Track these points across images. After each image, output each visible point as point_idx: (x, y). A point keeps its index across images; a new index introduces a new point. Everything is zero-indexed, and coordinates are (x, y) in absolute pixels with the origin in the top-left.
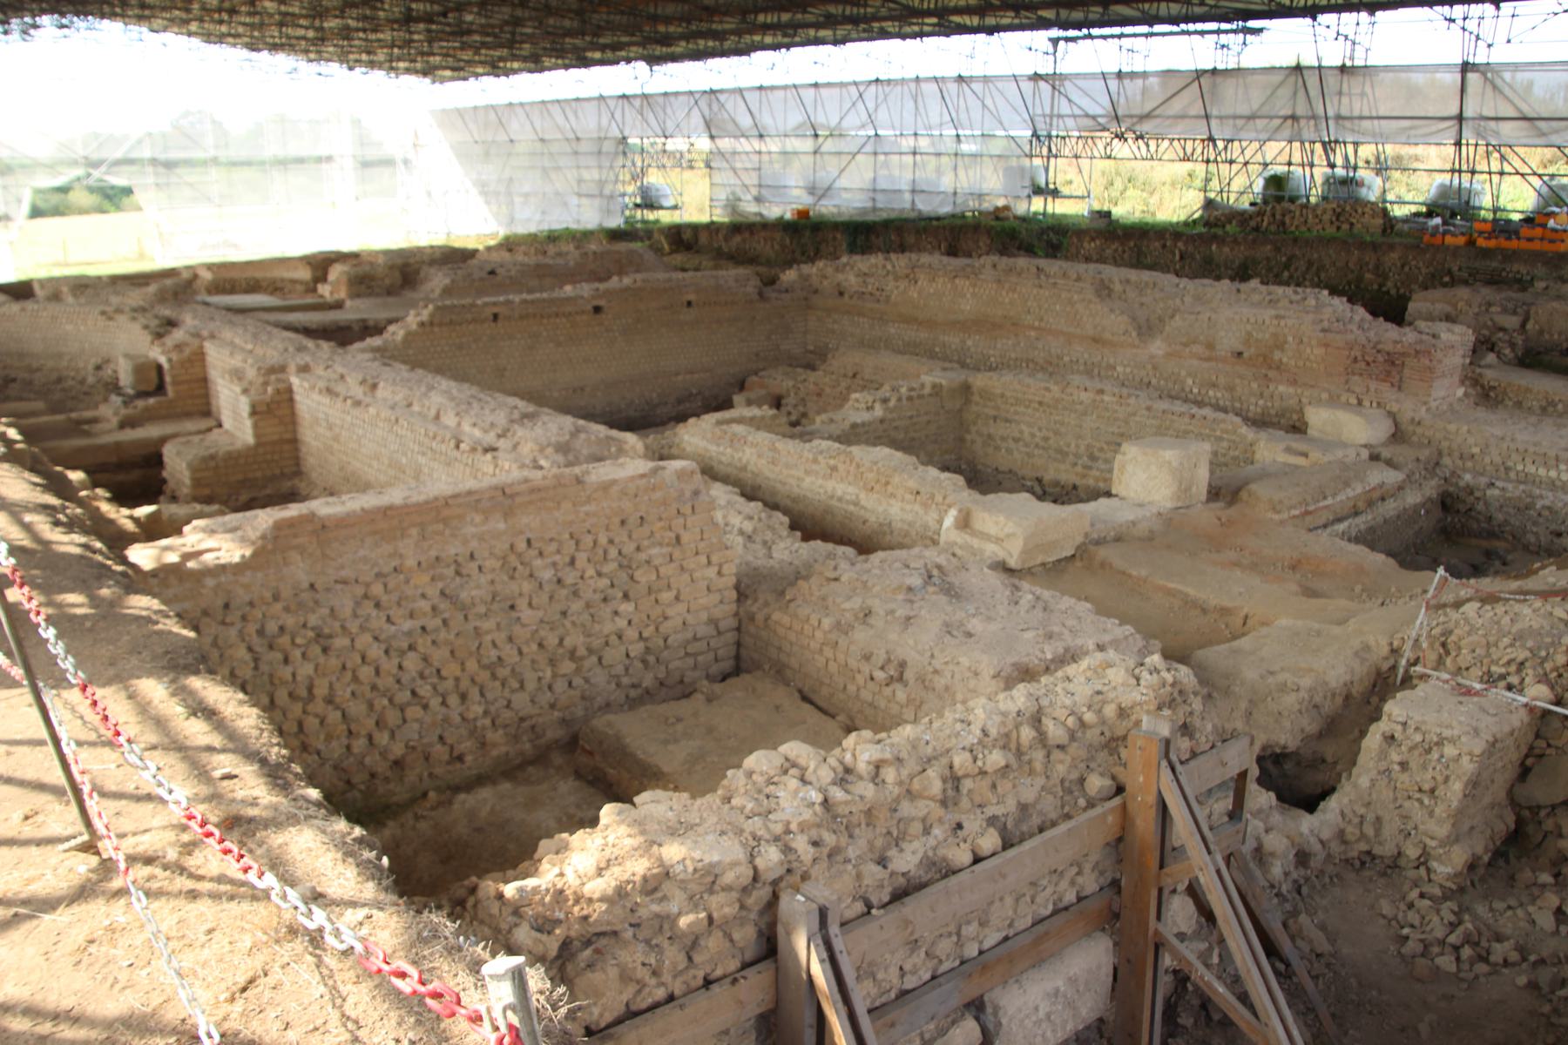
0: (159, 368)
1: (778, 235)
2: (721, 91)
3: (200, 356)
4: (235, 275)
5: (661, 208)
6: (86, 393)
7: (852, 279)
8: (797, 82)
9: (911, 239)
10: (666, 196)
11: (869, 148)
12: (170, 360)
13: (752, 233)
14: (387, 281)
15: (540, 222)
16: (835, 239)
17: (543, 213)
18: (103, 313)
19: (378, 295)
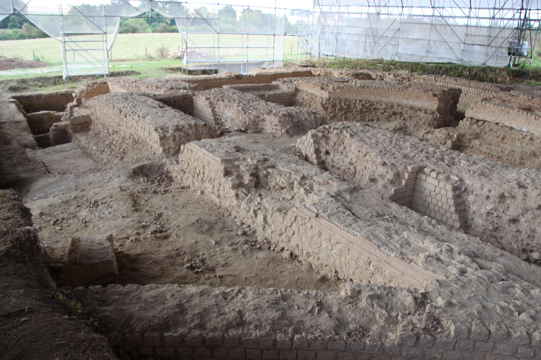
4: (351, 96)
15: (423, 57)
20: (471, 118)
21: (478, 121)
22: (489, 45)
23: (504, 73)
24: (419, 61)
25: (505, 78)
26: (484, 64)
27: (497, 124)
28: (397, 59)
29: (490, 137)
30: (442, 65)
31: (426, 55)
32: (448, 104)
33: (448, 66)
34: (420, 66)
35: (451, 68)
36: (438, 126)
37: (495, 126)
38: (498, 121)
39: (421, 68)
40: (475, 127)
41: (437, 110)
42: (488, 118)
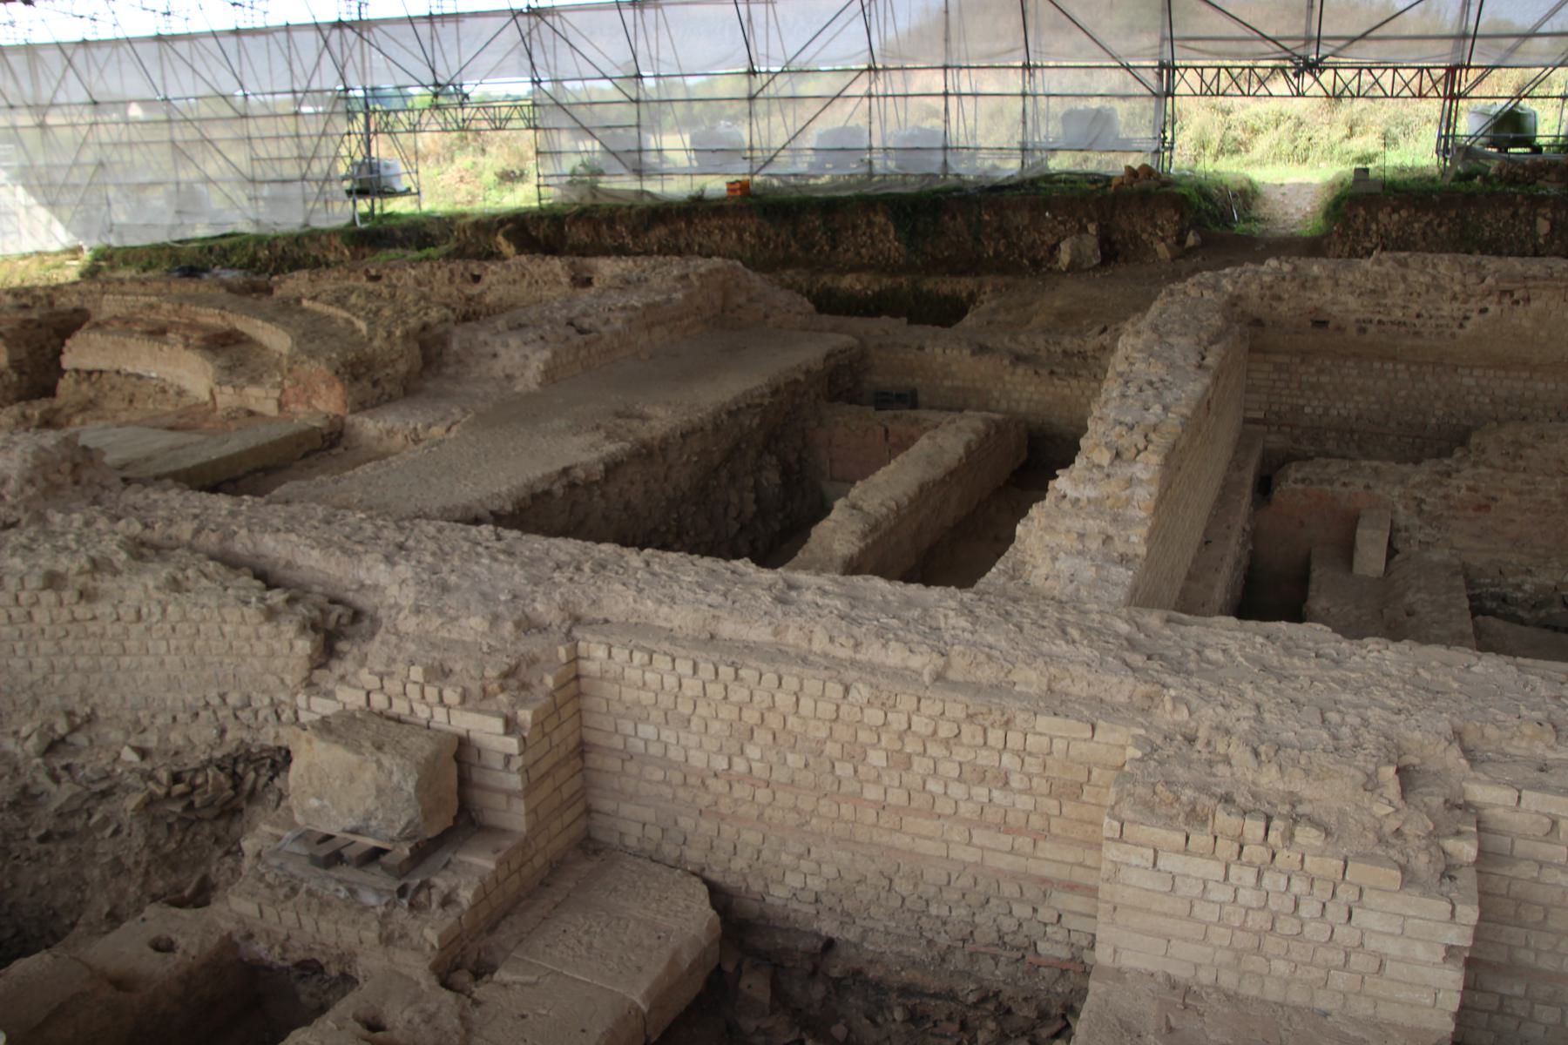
0: (463, 750)
1: (751, 224)
2: (552, 11)
3: (574, 681)
5: (394, 194)
6: (45, 838)
7: (1352, 302)
8: (130, 35)
9: (1021, 219)
10: (398, 175)
11: (861, 87)
12: (511, 726)
13: (689, 223)
14: (402, 367)
15: (172, 228)
16: (870, 224)
17: (179, 212)
18: (53, 580)
19: (391, 399)
20: (77, 371)
21: (90, 373)
22: (303, 178)
23: (337, 241)
24: (166, 240)
25: (343, 253)
26: (306, 225)
27: (118, 372)
28: (114, 242)
29: (113, 403)
30: (211, 243)
31: (177, 221)
32: (43, 347)
33: (225, 243)
34: (168, 251)
35: (233, 248)
36: (19, 399)
37: (116, 379)
38: (116, 367)
39: (170, 257)
40: (85, 386)
41: (12, 367)
42: (102, 365)
